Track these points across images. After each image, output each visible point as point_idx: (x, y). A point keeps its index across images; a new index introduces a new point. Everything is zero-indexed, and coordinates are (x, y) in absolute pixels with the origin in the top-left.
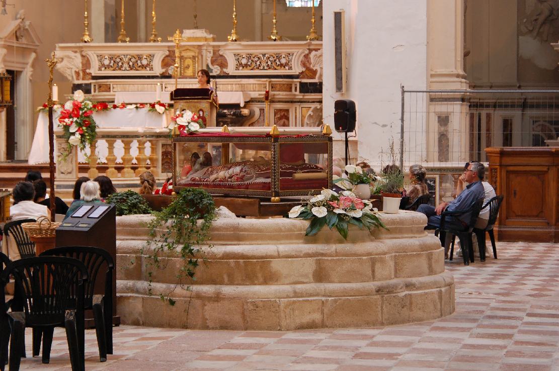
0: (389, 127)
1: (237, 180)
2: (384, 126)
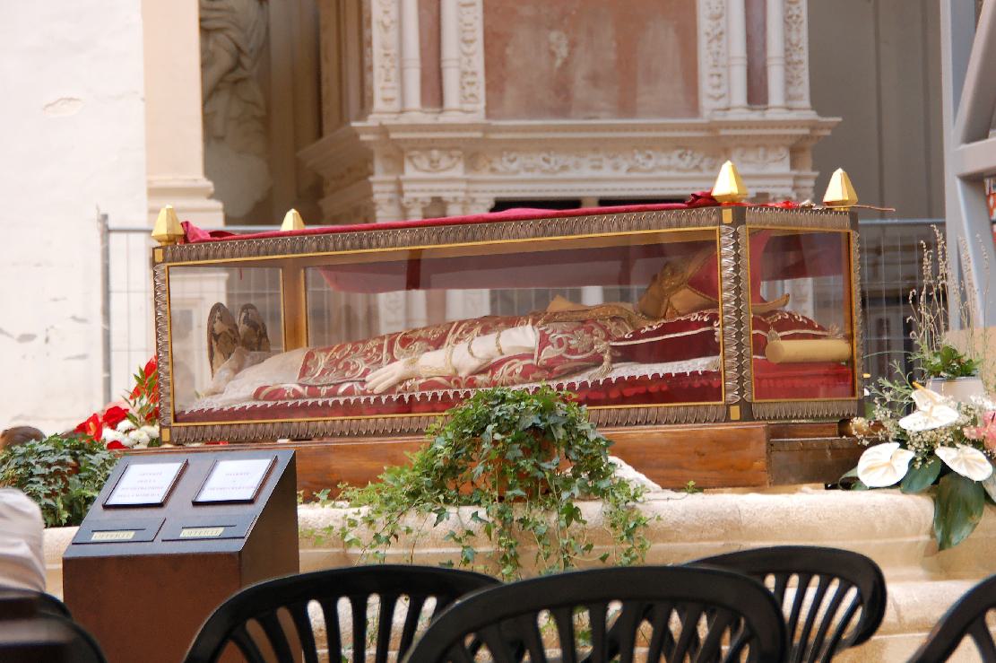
0: (40, 340)
1: (525, 375)
2: (27, 338)
